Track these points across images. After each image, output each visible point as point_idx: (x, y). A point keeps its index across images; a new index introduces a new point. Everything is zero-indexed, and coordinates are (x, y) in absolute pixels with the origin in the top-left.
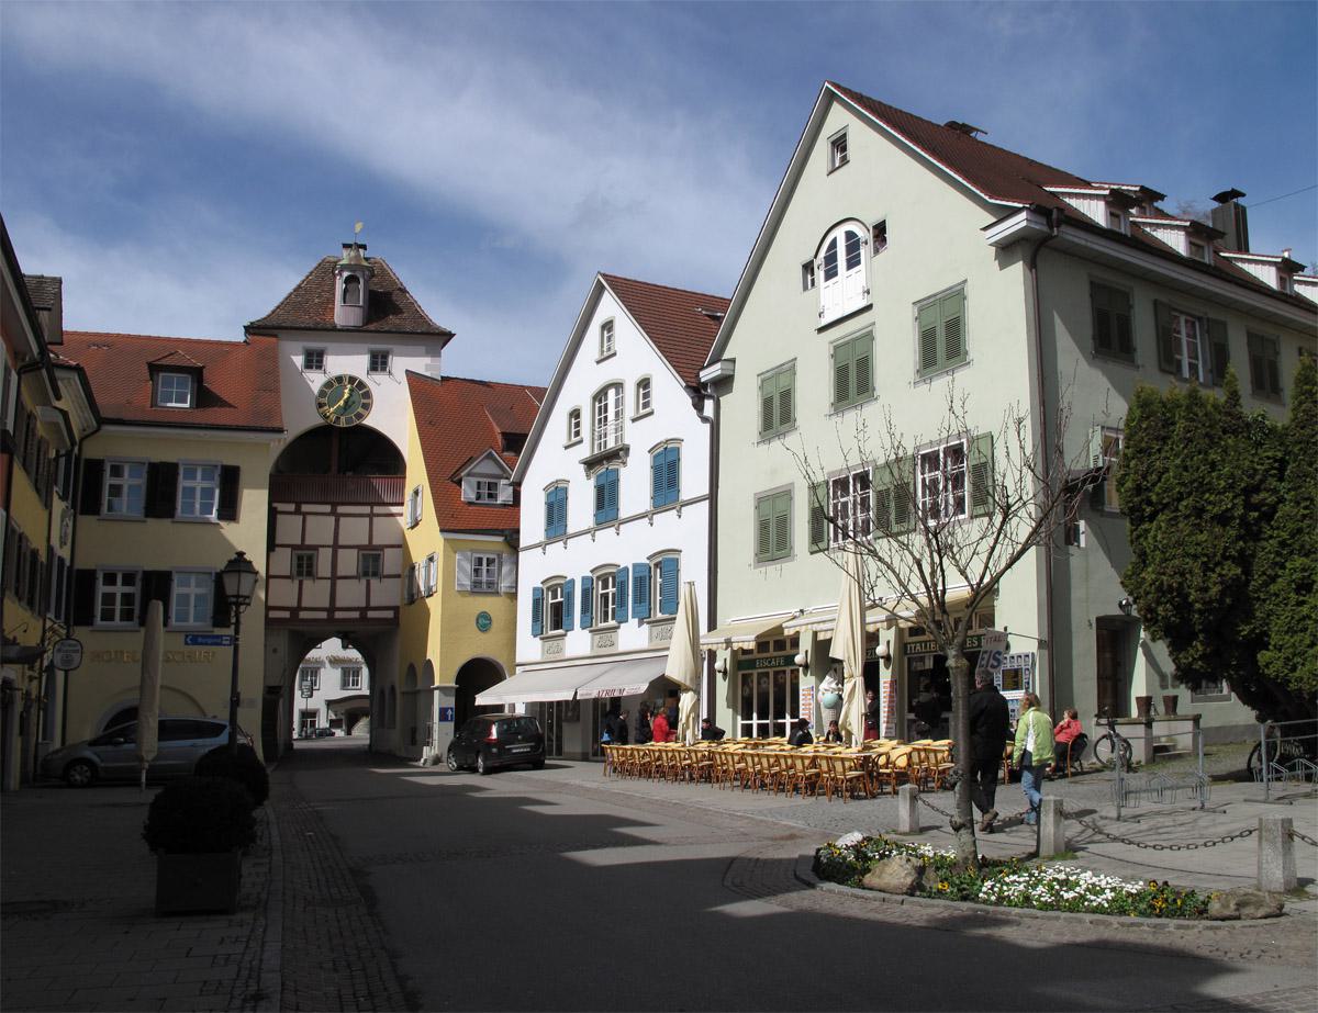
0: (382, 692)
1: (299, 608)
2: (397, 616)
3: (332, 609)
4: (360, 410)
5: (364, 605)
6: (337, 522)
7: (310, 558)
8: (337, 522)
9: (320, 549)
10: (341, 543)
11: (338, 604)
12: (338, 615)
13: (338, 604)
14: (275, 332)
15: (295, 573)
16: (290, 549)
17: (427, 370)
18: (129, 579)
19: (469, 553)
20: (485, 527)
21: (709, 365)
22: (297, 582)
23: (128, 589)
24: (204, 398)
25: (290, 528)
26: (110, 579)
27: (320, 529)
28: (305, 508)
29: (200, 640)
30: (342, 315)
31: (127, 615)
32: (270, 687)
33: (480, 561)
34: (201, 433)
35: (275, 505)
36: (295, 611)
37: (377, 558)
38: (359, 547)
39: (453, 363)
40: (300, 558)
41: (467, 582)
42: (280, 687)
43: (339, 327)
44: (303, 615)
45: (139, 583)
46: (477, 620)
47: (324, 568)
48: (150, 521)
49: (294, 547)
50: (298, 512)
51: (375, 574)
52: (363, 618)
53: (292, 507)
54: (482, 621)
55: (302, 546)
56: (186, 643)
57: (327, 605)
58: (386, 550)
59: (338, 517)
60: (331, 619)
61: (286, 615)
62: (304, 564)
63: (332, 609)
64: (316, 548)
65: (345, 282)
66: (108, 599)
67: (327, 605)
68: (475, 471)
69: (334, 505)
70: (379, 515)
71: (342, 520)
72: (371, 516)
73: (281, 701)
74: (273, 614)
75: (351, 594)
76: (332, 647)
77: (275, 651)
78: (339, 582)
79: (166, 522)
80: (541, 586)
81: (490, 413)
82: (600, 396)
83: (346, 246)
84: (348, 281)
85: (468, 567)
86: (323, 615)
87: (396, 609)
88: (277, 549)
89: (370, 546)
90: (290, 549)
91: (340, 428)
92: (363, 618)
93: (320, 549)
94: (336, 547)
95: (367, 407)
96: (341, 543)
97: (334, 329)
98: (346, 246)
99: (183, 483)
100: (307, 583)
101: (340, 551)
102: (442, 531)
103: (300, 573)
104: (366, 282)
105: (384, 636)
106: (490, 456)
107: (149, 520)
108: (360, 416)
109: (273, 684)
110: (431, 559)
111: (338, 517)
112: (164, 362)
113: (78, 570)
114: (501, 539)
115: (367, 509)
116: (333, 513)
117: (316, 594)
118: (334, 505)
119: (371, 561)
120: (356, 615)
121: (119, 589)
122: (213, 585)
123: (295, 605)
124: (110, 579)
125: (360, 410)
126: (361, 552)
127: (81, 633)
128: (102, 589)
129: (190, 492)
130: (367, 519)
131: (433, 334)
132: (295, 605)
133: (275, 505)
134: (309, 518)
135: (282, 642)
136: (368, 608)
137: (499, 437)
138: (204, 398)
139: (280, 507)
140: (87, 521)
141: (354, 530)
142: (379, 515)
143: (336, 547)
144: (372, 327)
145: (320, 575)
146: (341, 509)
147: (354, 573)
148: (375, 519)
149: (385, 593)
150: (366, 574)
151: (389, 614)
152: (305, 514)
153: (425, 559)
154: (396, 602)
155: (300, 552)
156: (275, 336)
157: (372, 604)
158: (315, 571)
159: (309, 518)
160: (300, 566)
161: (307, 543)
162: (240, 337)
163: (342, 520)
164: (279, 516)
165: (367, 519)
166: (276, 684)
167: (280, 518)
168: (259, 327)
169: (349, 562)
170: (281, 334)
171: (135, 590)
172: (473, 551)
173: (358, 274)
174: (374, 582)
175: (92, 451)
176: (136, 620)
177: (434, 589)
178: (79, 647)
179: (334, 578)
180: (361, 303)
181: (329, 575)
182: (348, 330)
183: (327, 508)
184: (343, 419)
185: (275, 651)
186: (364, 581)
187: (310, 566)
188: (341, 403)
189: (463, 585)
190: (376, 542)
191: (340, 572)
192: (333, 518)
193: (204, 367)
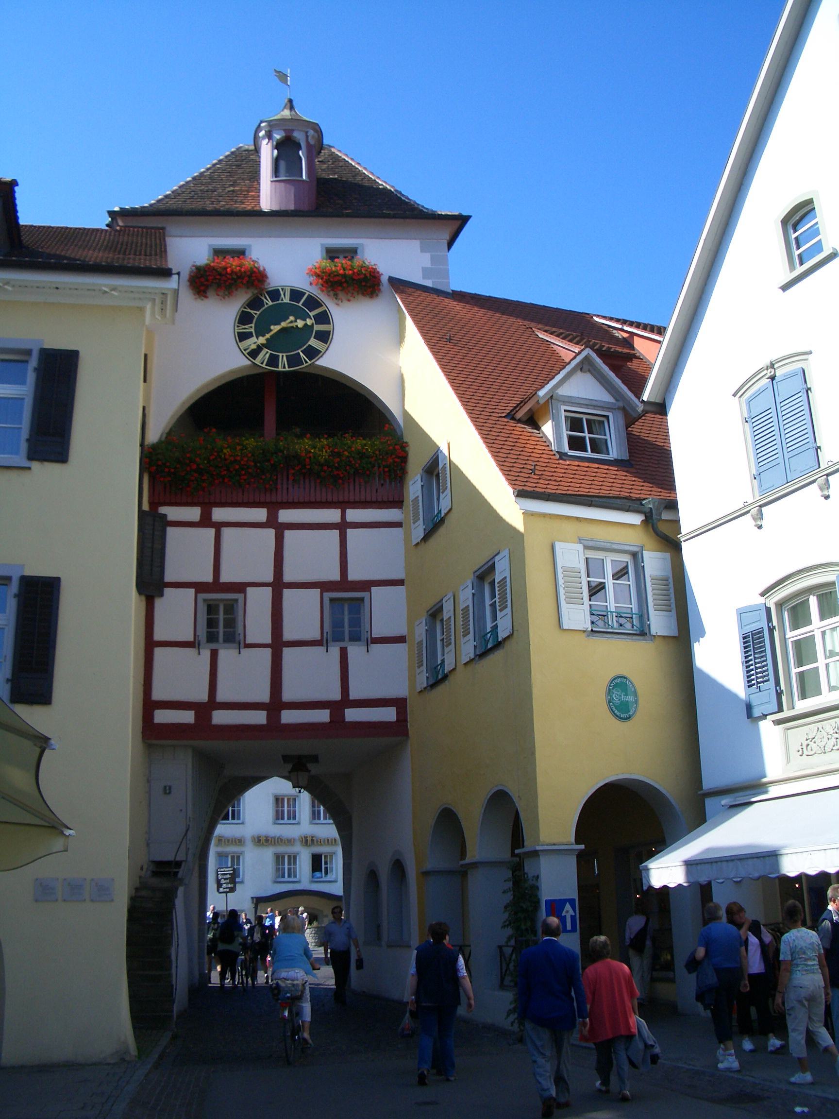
0: (373, 876)
1: (213, 704)
3: (276, 704)
4: (313, 342)
7: (230, 608)
10: (288, 577)
11: (288, 695)
12: (288, 717)
13: (288, 695)
16: (193, 591)
17: (424, 277)
22: (206, 654)
25: (188, 552)
27: (247, 551)
28: (219, 514)
35: (163, 510)
36: (203, 710)
38: (324, 586)
40: (211, 609)
42: (178, 864)
46: (609, 692)
47: (256, 620)
49: (199, 587)
50: (206, 521)
51: (355, 638)
52: (337, 721)
53: (194, 513)
55: (216, 585)
57: (264, 696)
59: (281, 529)
61: (188, 717)
63: (276, 704)
64: (240, 588)
67: (264, 696)
68: (563, 391)
69: (273, 508)
71: (288, 534)
72: (343, 527)
73: (181, 891)
74: (162, 716)
75: (311, 676)
77: (167, 790)
78: (287, 652)
80: (762, 600)
86: (259, 718)
87: (400, 704)
88: (167, 591)
89: (344, 584)
90: (193, 591)
91: (279, 372)
92: (337, 721)
95: (325, 337)
96: (288, 577)
100: (227, 655)
101: (287, 592)
103: (212, 638)
108: (313, 353)
111: (281, 529)
114: (636, 519)
115: (332, 515)
116: (271, 522)
118: (273, 508)
120: (323, 716)
123: (204, 697)
125: (313, 342)
126: (328, 595)
130: (336, 533)
133: (163, 510)
134: (226, 532)
136: (346, 702)
139: (173, 513)
143: (278, 585)
146: (286, 516)
147: (314, 634)
148: (350, 532)
150: (338, 637)
151: (389, 714)
152: (219, 527)
154: (399, 690)
157: (354, 695)
158: (240, 630)
159: (226, 532)
160: (211, 623)
161: (225, 578)
163: (288, 534)
164: (171, 531)
165: (336, 533)
166: (170, 858)
169: (304, 614)
173: (298, 136)
174: (355, 652)
179: (278, 644)
181: (268, 640)
183: (260, 514)
184: (283, 358)
185: (167, 790)
186: (335, 651)
187: (230, 623)
190: (354, 575)
192: (271, 533)
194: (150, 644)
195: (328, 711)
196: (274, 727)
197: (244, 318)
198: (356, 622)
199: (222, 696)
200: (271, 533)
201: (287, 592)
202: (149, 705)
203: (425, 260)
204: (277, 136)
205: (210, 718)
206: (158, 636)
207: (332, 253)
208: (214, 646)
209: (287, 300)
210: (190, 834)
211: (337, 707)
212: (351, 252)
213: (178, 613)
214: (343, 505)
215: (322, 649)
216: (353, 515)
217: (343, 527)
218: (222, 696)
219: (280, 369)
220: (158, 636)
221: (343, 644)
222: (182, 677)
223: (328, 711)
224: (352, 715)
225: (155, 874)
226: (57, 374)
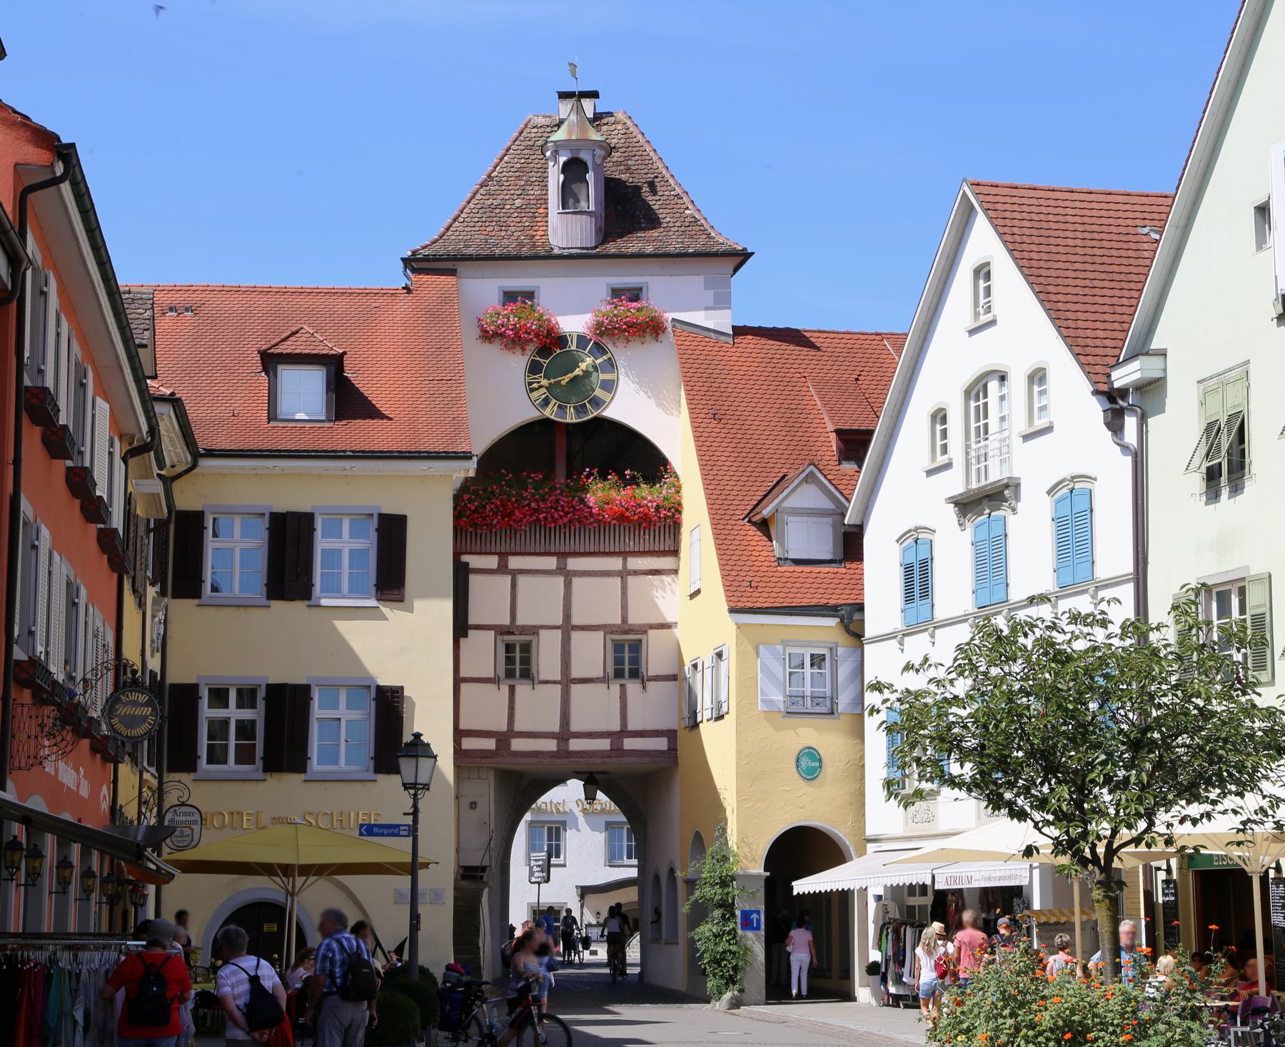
0: (657, 878)
2: (672, 750)
3: (564, 734)
5: (618, 728)
6: (568, 586)
7: (526, 648)
8: (568, 586)
9: (542, 632)
10: (576, 621)
11: (575, 727)
12: (575, 745)
13: (575, 727)
14: (449, 265)
15: (502, 673)
18: (247, 697)
19: (780, 648)
20: (805, 602)
21: (1131, 358)
22: (505, 689)
23: (246, 714)
24: (347, 400)
25: (489, 597)
26: (219, 696)
28: (515, 562)
29: (375, 830)
31: (245, 756)
32: (466, 868)
34: (347, 464)
35: (465, 558)
36: (504, 738)
37: (636, 647)
39: (758, 298)
40: (509, 648)
41: (778, 697)
42: (483, 869)
43: (556, 251)
44: (518, 745)
45: (261, 703)
48: (276, 605)
49: (501, 631)
50: (503, 569)
51: (635, 674)
52: (617, 750)
53: (492, 562)
54: (805, 762)
56: (361, 834)
57: (556, 728)
58: (651, 632)
59: (569, 576)
60: (563, 753)
61: (490, 744)
62: (517, 660)
63: (564, 734)
64: (534, 630)
65: (563, 172)
66: (218, 729)
67: (556, 728)
68: (785, 505)
69: (562, 556)
70: (636, 573)
71: (576, 582)
72: (624, 574)
73: (486, 891)
74: (468, 743)
75: (596, 710)
76: (569, 794)
77: (473, 805)
78: (575, 689)
79: (298, 607)
81: (819, 393)
82: (976, 390)
83: (564, 96)
84: (566, 168)
85: (780, 671)
86: (551, 745)
87: (671, 735)
88: (471, 632)
89: (624, 628)
91: (567, 424)
92: (617, 750)
93: (542, 632)
94: (567, 628)
96: (576, 621)
97: (550, 257)
98: (564, 96)
99: (321, 544)
100: (523, 689)
102: (733, 610)
103: (510, 674)
104: (598, 168)
105: (647, 785)
106: (810, 478)
107: (274, 603)
108: (597, 403)
109: (475, 862)
110: (719, 655)
111: (569, 576)
112: (285, 348)
113: (172, 685)
114: (832, 622)
115: (615, 563)
116: (561, 570)
117: (537, 709)
118: (562, 556)
119: (627, 657)
120: (605, 744)
121: (234, 713)
122: (373, 704)
123: (504, 728)
125: (598, 392)
126: (609, 637)
128: (207, 712)
131: (716, 255)
132: (504, 728)
133: (465, 558)
134: (522, 580)
135: (485, 791)
136: (624, 733)
137: (833, 436)
138: (347, 400)
139: (474, 561)
140: (183, 608)
141: (597, 598)
142: (636, 573)
143: (567, 628)
144: (611, 248)
145: (543, 677)
146: (574, 564)
148: (631, 580)
149: (649, 708)
150: (619, 674)
151: (661, 744)
153: (713, 653)
155: (509, 638)
156: (452, 272)
157: (632, 726)
158: (534, 670)
159: (522, 580)
160: (510, 660)
161: (520, 621)
162: (397, 278)
163: (576, 582)
166: (478, 864)
167: (473, 579)
168: (426, 259)
169: (591, 654)
170: (460, 267)
172: (785, 643)
173: (585, 156)
174: (633, 687)
175: (187, 499)
176: (259, 762)
177: (724, 709)
178: (197, 817)
179: (567, 681)
180: (592, 208)
181: (558, 678)
182: (571, 257)
183: (550, 563)
185: (473, 805)
186: (615, 687)
187: (526, 661)
188: (565, 379)
189: (772, 701)
190: (633, 619)
191: (576, 673)
192: (560, 580)
193: (345, 353)
194: (458, 681)
195: (609, 741)
196: (563, 753)
197: (534, 368)
198: (635, 660)
199: (518, 727)
200: (560, 580)
201: (575, 636)
204: (562, 159)
205: (509, 746)
206: (463, 674)
207: (616, 293)
208: (511, 682)
209: (574, 347)
210: (492, 844)
212: (635, 294)
213: (483, 653)
214: (624, 554)
215: (603, 686)
216: (636, 563)
217: (624, 574)
218: (518, 727)
219: (568, 421)
220: (463, 674)
221: (623, 682)
223: (609, 741)
224: (630, 744)
225: (464, 877)
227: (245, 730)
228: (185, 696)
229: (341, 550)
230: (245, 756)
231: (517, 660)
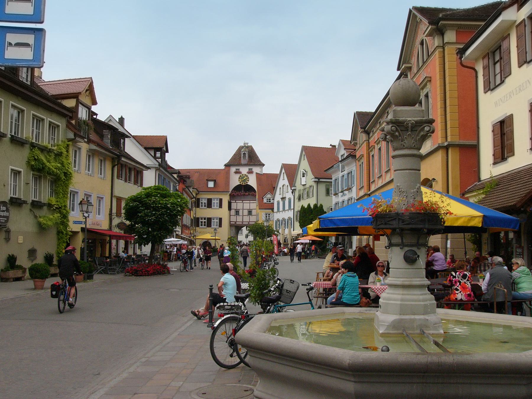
18: (205, 219)
25: (234, 206)
26: (202, 219)
30: (243, 161)
31: (205, 225)
33: (266, 214)
36: (236, 222)
41: (264, 219)
47: (241, 213)
62: (237, 213)
66: (202, 222)
75: (246, 219)
82: (283, 186)
85: (265, 216)
94: (243, 209)
99: (213, 201)
100: (238, 216)
117: (239, 219)
121: (203, 221)
124: (202, 219)
127: (197, 228)
128: (200, 220)
129: (214, 203)
135: (234, 229)
143: (243, 209)
169: (246, 212)
171: (206, 221)
179: (243, 216)
202: (230, 222)
203: (260, 170)
211: (249, 222)
213: (233, 212)
222: (233, 219)
226: (221, 200)
227: (205, 222)
228: (198, 219)
229: (215, 202)
230: (205, 225)
231: (237, 213)
